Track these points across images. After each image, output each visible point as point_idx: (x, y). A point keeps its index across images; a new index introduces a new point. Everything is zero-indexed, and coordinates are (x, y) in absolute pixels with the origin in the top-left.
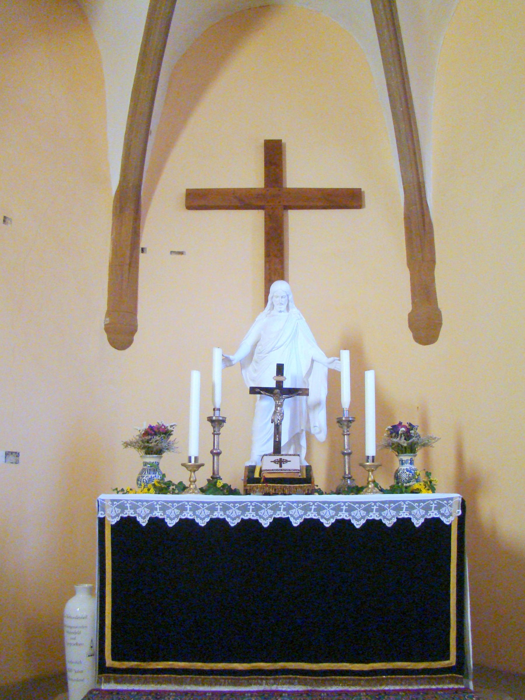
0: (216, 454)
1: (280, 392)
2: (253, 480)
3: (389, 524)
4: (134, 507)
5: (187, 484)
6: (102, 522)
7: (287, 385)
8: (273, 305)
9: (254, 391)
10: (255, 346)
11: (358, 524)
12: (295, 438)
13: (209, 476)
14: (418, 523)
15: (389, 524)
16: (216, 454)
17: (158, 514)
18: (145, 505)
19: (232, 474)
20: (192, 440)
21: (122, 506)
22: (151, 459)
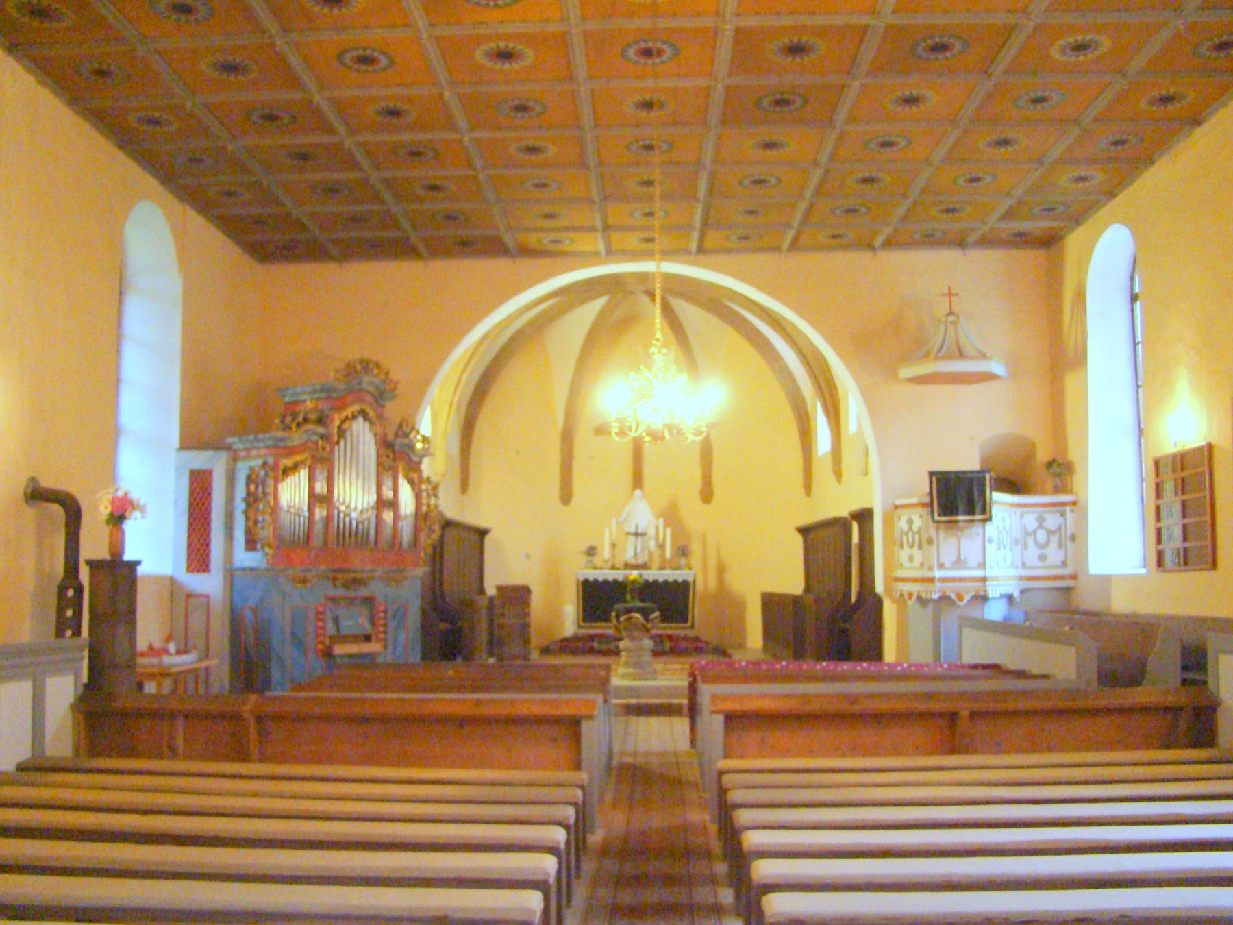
1: (636, 534)
2: (627, 566)
12: (643, 551)
18: (592, 575)
20: (606, 552)
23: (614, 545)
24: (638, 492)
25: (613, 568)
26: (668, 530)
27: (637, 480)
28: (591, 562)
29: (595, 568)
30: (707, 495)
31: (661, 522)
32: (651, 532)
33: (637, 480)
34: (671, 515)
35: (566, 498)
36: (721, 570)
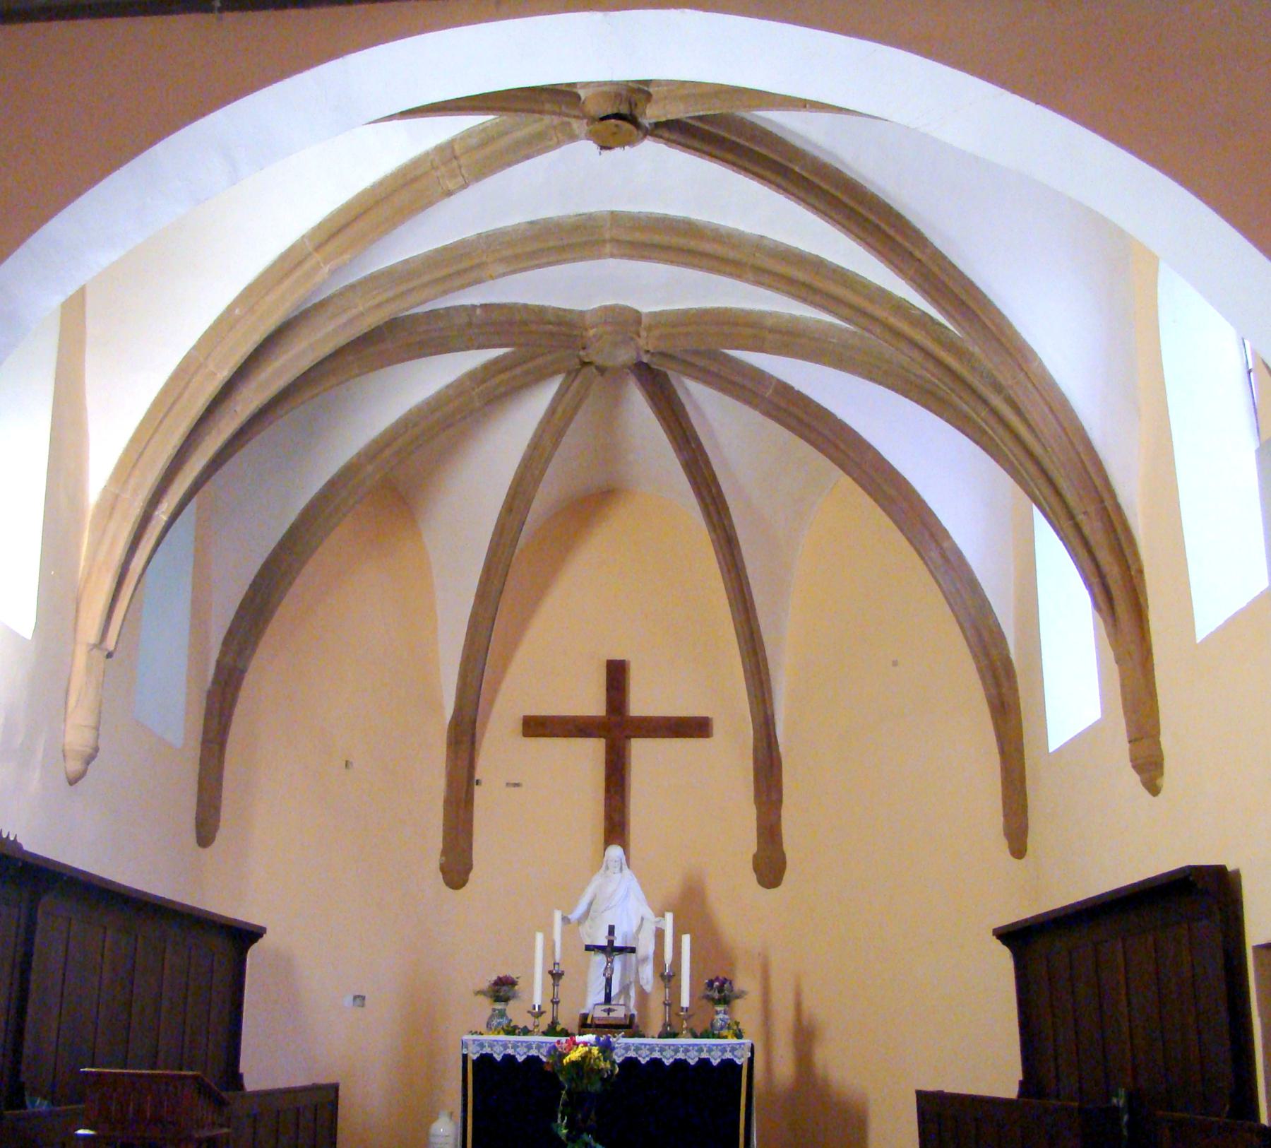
0: (555, 1002)
1: (610, 950)
3: (692, 1062)
4: (491, 1046)
5: (531, 1028)
6: (465, 1057)
7: (617, 943)
8: (607, 868)
9: (588, 948)
10: (591, 904)
11: (667, 1062)
12: (625, 989)
13: (550, 1020)
14: (715, 1062)
15: (692, 1062)
16: (555, 1002)
17: (510, 1051)
18: (499, 1045)
19: (568, 1019)
20: (537, 991)
21: (482, 1045)
22: (499, 1006)
23: (556, 976)
24: (615, 851)
25: (552, 1030)
26: (686, 939)
27: (616, 828)
28: (502, 1014)
29: (511, 1031)
30: (770, 868)
31: (668, 922)
32: (646, 946)
33: (616, 828)
34: (690, 908)
35: (456, 869)
36: (805, 1037)
